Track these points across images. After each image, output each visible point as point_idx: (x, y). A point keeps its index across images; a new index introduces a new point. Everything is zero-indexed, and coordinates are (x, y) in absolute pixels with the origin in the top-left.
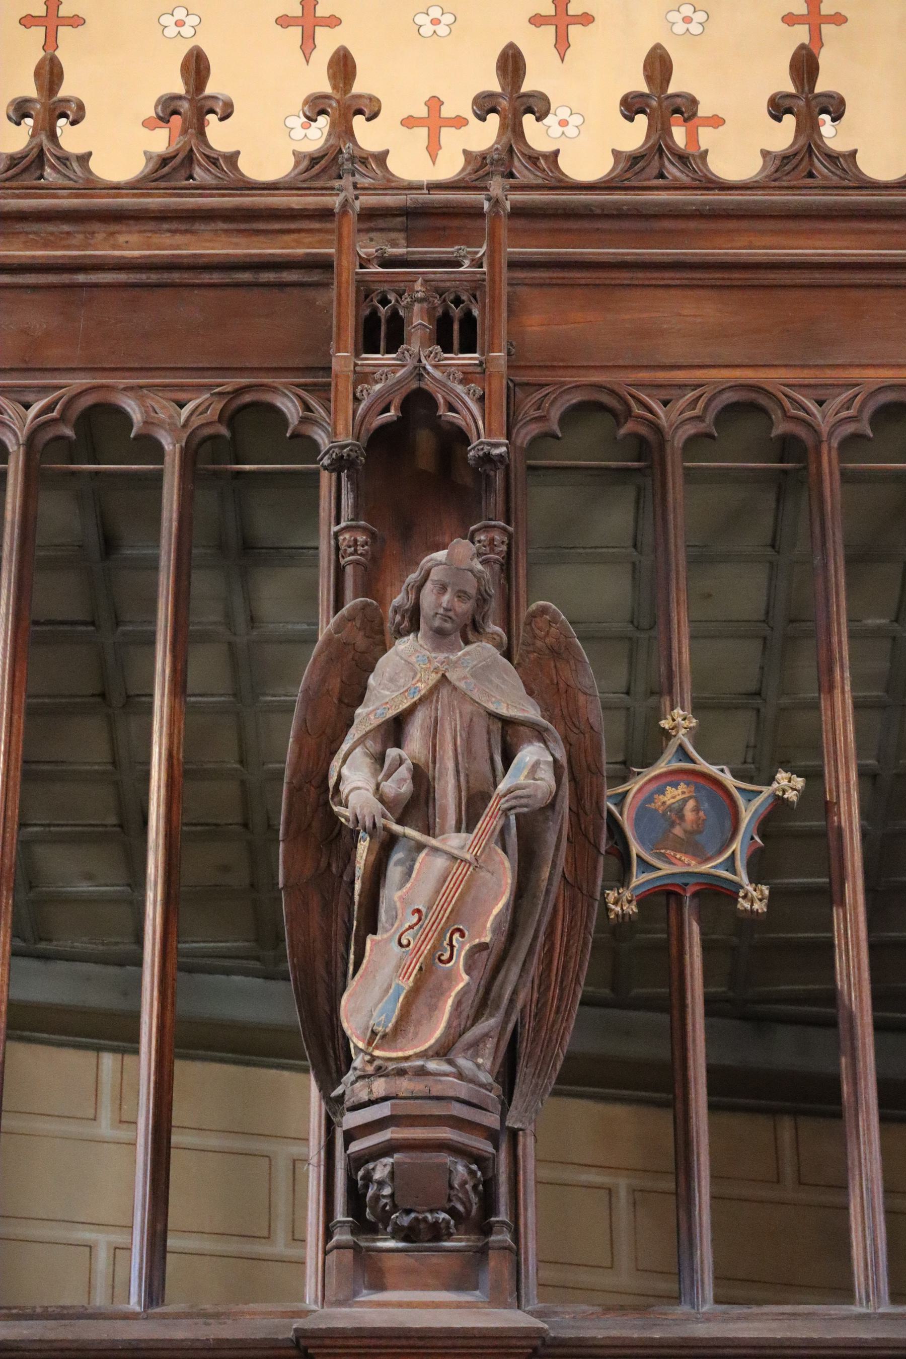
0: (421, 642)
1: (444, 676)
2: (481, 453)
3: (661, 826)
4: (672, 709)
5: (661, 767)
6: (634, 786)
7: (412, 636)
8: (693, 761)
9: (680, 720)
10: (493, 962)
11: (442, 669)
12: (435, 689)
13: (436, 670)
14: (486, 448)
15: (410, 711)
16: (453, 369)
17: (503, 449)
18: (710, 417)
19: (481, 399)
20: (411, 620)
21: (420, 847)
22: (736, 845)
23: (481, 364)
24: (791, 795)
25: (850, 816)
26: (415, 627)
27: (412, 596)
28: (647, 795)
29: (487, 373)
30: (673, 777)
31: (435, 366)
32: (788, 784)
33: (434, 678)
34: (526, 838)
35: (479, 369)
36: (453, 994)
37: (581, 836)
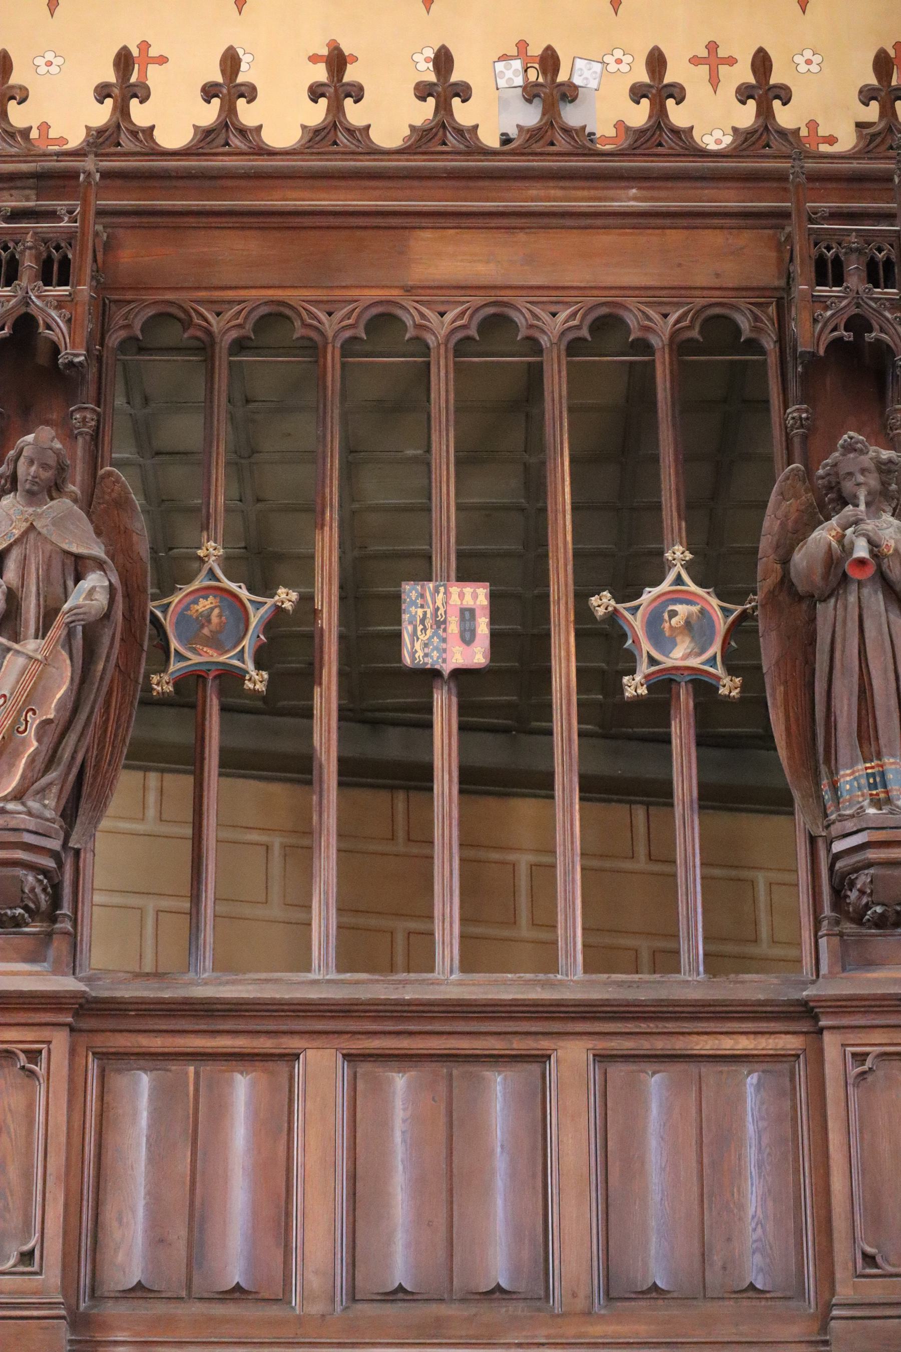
0: (18, 499)
1: (32, 524)
2: (66, 361)
3: (193, 627)
4: (208, 541)
5: (196, 585)
6: (175, 599)
7: (12, 494)
8: (218, 580)
9: (212, 550)
10: (57, 733)
11: (31, 519)
12: (25, 533)
13: (26, 520)
14: (70, 357)
15: (8, 549)
16: (50, 298)
17: (82, 358)
18: (249, 326)
19: (69, 321)
20: (11, 484)
21: (9, 650)
22: (246, 642)
23: (70, 295)
24: (287, 605)
25: (329, 620)
26: (14, 488)
27: (11, 467)
28: (188, 604)
29: (75, 301)
30: (205, 592)
31: (38, 297)
32: (286, 597)
33: (25, 525)
34: (88, 639)
35: (69, 299)
36: (26, 755)
37: (131, 637)
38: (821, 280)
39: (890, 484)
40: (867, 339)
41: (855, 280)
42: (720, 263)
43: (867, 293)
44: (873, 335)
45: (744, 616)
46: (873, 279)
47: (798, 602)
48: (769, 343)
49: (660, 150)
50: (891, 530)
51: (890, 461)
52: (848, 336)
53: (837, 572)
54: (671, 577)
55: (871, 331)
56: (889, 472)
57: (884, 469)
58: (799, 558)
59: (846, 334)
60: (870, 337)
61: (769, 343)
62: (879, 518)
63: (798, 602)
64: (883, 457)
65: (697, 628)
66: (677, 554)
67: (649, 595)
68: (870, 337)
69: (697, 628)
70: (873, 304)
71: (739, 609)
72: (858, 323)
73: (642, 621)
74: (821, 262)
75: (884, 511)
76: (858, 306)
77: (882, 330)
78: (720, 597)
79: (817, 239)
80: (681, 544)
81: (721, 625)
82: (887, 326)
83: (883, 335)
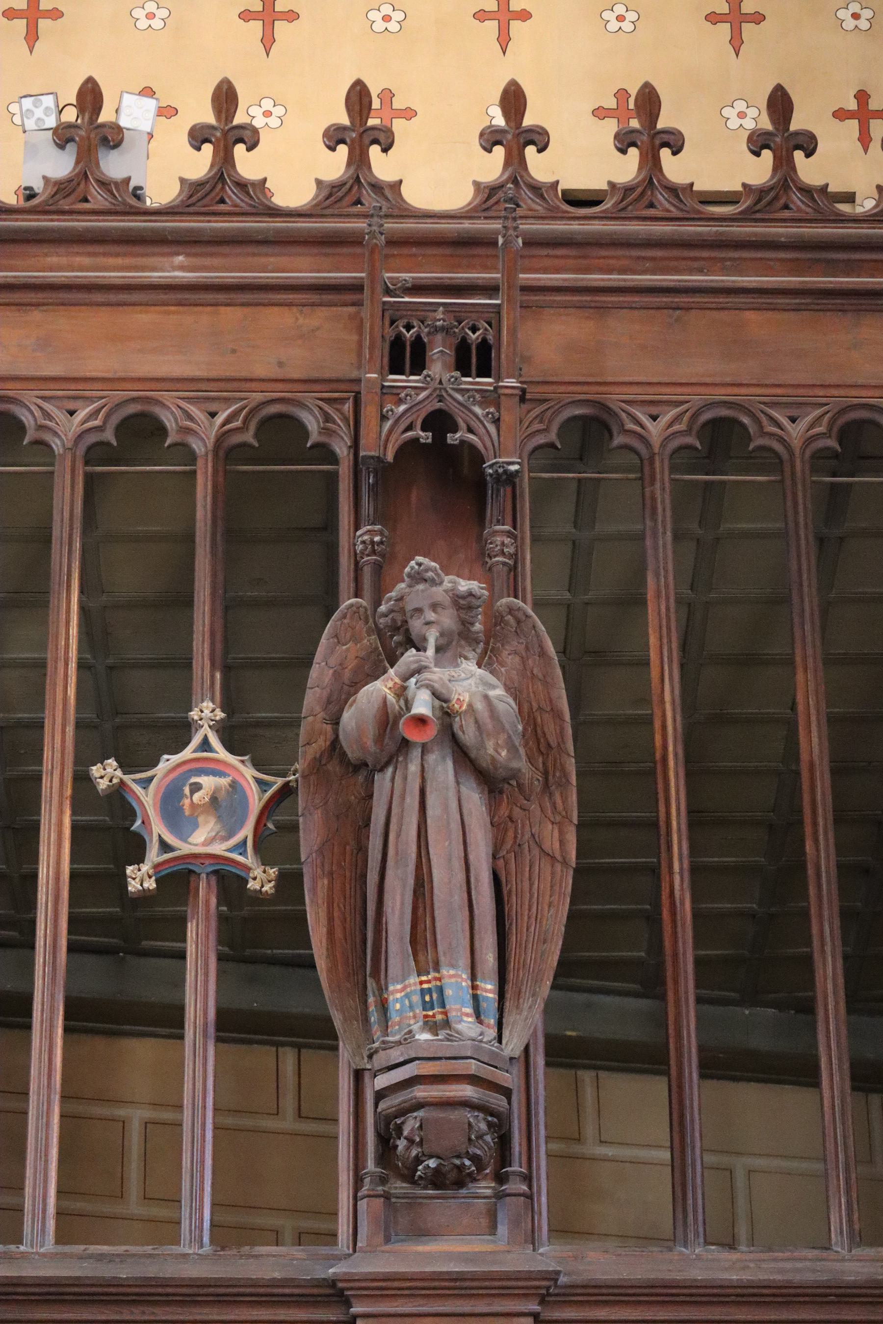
38: (396, 367)
39: (472, 624)
40: (449, 441)
41: (439, 365)
42: (287, 348)
43: (453, 384)
44: (458, 435)
45: (287, 791)
46: (462, 365)
47: (350, 772)
48: (341, 449)
49: (222, 207)
50: (471, 681)
51: (471, 594)
52: (426, 437)
53: (393, 737)
54: (196, 740)
55: (455, 431)
56: (470, 608)
57: (463, 604)
58: (348, 717)
59: (421, 433)
60: (452, 439)
61: (341, 449)
62: (457, 666)
63: (350, 772)
64: (461, 589)
65: (226, 806)
66: (206, 712)
67: (168, 762)
68: (452, 439)
69: (226, 806)
70: (459, 397)
71: (280, 781)
72: (439, 421)
73: (155, 795)
74: (397, 344)
75: (466, 658)
76: (441, 399)
77: (470, 430)
78: (257, 765)
79: (392, 315)
80: (213, 701)
81: (256, 801)
82: (475, 424)
83: (471, 436)
